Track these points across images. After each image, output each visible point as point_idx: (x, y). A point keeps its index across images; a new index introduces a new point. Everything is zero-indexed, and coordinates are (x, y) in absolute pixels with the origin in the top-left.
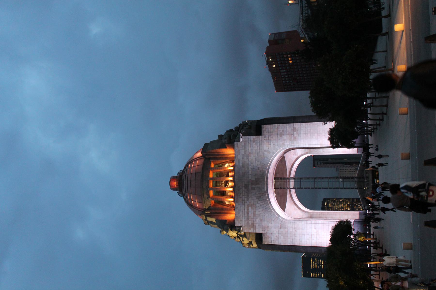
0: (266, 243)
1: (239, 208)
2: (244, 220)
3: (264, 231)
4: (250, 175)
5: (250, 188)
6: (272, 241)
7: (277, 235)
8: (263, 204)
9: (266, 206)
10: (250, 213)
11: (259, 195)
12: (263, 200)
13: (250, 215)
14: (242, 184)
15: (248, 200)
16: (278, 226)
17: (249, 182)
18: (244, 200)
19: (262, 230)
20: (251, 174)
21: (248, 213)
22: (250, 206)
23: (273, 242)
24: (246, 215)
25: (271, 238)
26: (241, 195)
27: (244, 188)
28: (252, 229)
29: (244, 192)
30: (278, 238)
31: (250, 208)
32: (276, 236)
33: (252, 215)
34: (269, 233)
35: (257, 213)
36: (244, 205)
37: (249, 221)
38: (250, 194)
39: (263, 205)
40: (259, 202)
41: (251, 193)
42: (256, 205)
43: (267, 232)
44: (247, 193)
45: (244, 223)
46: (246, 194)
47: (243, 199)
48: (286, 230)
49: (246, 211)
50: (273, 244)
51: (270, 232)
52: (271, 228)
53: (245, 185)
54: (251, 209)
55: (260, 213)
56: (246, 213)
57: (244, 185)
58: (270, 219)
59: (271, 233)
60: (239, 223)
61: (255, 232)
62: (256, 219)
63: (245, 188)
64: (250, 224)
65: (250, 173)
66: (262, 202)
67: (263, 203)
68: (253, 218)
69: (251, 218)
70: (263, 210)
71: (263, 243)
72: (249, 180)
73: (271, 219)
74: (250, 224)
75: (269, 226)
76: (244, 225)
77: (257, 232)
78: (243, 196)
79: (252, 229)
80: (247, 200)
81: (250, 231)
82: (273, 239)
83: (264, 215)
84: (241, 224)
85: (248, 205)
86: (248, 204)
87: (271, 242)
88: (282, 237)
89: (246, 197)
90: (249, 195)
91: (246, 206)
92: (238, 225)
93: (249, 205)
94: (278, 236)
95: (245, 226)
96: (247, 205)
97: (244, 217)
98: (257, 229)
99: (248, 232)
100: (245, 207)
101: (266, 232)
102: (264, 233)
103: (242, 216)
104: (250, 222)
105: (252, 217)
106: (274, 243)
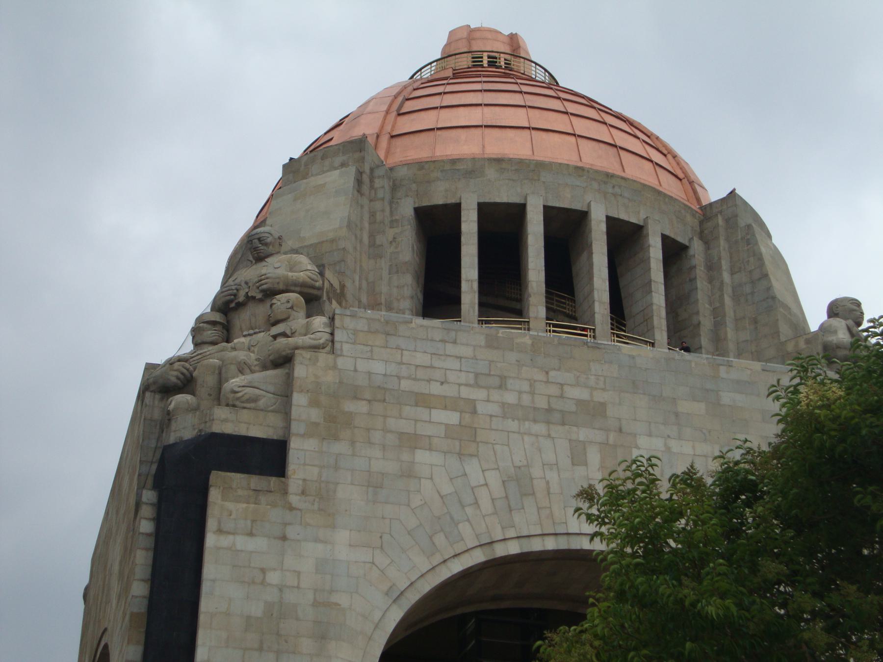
0: (214, 495)
1: (450, 349)
2: (378, 367)
3: (303, 493)
4: (665, 445)
5: (583, 434)
6: (231, 537)
7: (273, 578)
8: (480, 502)
9: (468, 520)
10: (422, 413)
11: (539, 485)
12: (511, 511)
13: (408, 410)
14: (604, 390)
15: (507, 412)
16: (331, 591)
17: (620, 430)
18: (502, 386)
19: (304, 480)
20: (668, 449)
21: (423, 400)
22: (467, 416)
23: (225, 541)
24: (405, 385)
25: (251, 534)
26: (541, 376)
27: (582, 394)
28: (315, 415)
29: (553, 390)
30: (254, 582)
31: (453, 418)
32: (263, 571)
33: (405, 426)
34: (285, 524)
35: (422, 456)
36: (472, 382)
37: (369, 401)
38: (540, 428)
39: (476, 503)
40: (494, 480)
41: (549, 436)
42: (471, 455)
43: (291, 508)
44: (549, 410)
45: (356, 370)
46: (542, 403)
47: (510, 382)
48: (307, 645)
49: (436, 389)
50: (211, 540)
51: (291, 532)
52: (317, 540)
53: (603, 405)
54: (447, 425)
55: (420, 478)
56: (421, 388)
57: (599, 397)
58: (381, 537)
59: (284, 538)
60: (356, 332)
61: (295, 427)
62: (384, 447)
63: (579, 402)
64: (350, 406)
65: (674, 445)
66: (493, 500)
67: (486, 505)
68: (385, 430)
69: (385, 417)
70: (442, 497)
71: (216, 477)
72: (635, 435)
73: (382, 547)
74: (350, 406)
75: (333, 527)
76: (341, 362)
77: (295, 444)
78: (532, 383)
79: (315, 415)
80: (503, 405)
81: (299, 399)
82: (241, 542)
83: (409, 506)
84: (346, 347)
85: (475, 407)
86: (480, 408)
87: (220, 531)
88: (256, 610)
89: (526, 399)
90: (535, 421)
91: (465, 393)
92: (343, 328)
93: (474, 412)
94: (263, 583)
95: (335, 367)
96: (472, 403)
97: (392, 369)
98: (311, 444)
99: (297, 384)
100: (460, 385)
101: (294, 499)
102: (285, 492)
103: (401, 363)
104: (361, 407)
105: (392, 423)
106: (218, 548)
